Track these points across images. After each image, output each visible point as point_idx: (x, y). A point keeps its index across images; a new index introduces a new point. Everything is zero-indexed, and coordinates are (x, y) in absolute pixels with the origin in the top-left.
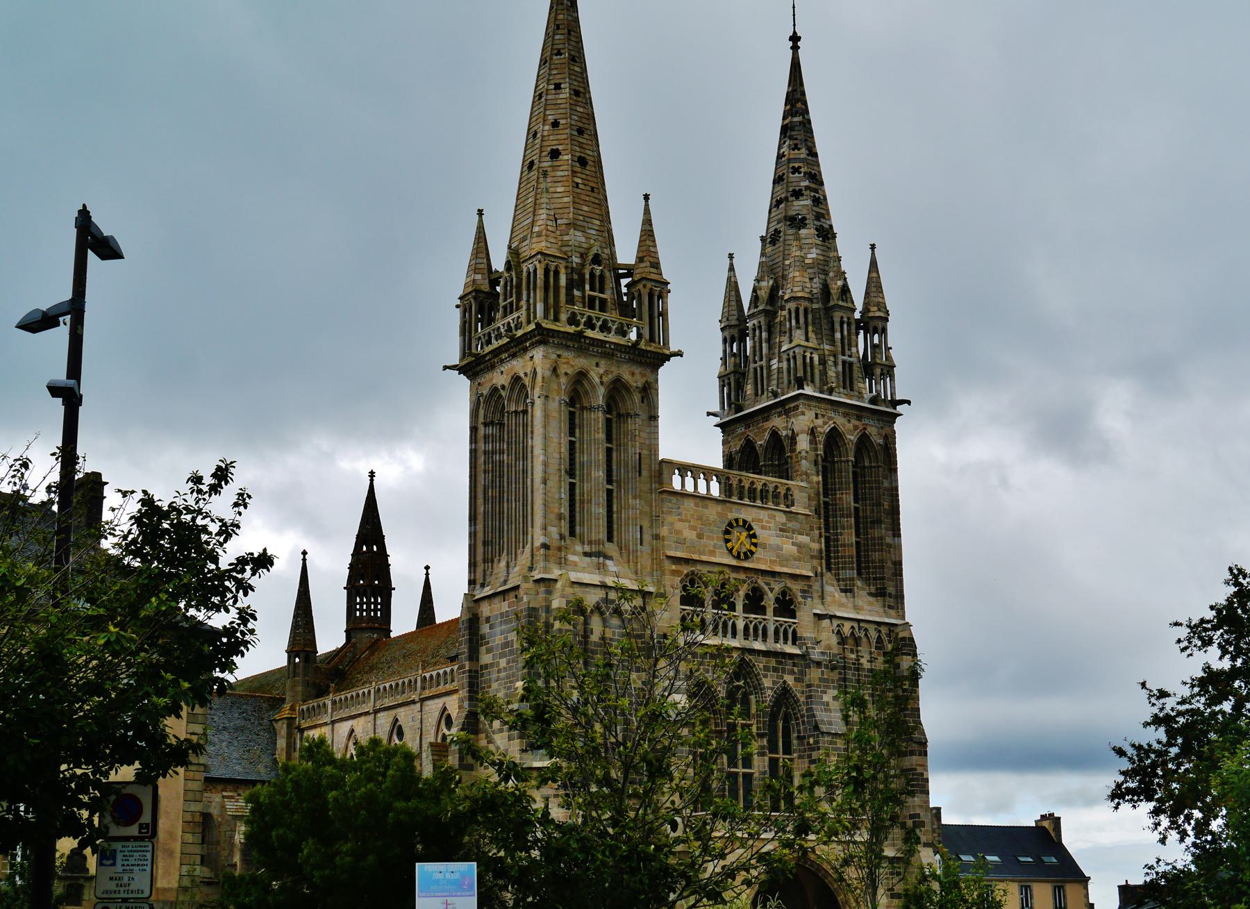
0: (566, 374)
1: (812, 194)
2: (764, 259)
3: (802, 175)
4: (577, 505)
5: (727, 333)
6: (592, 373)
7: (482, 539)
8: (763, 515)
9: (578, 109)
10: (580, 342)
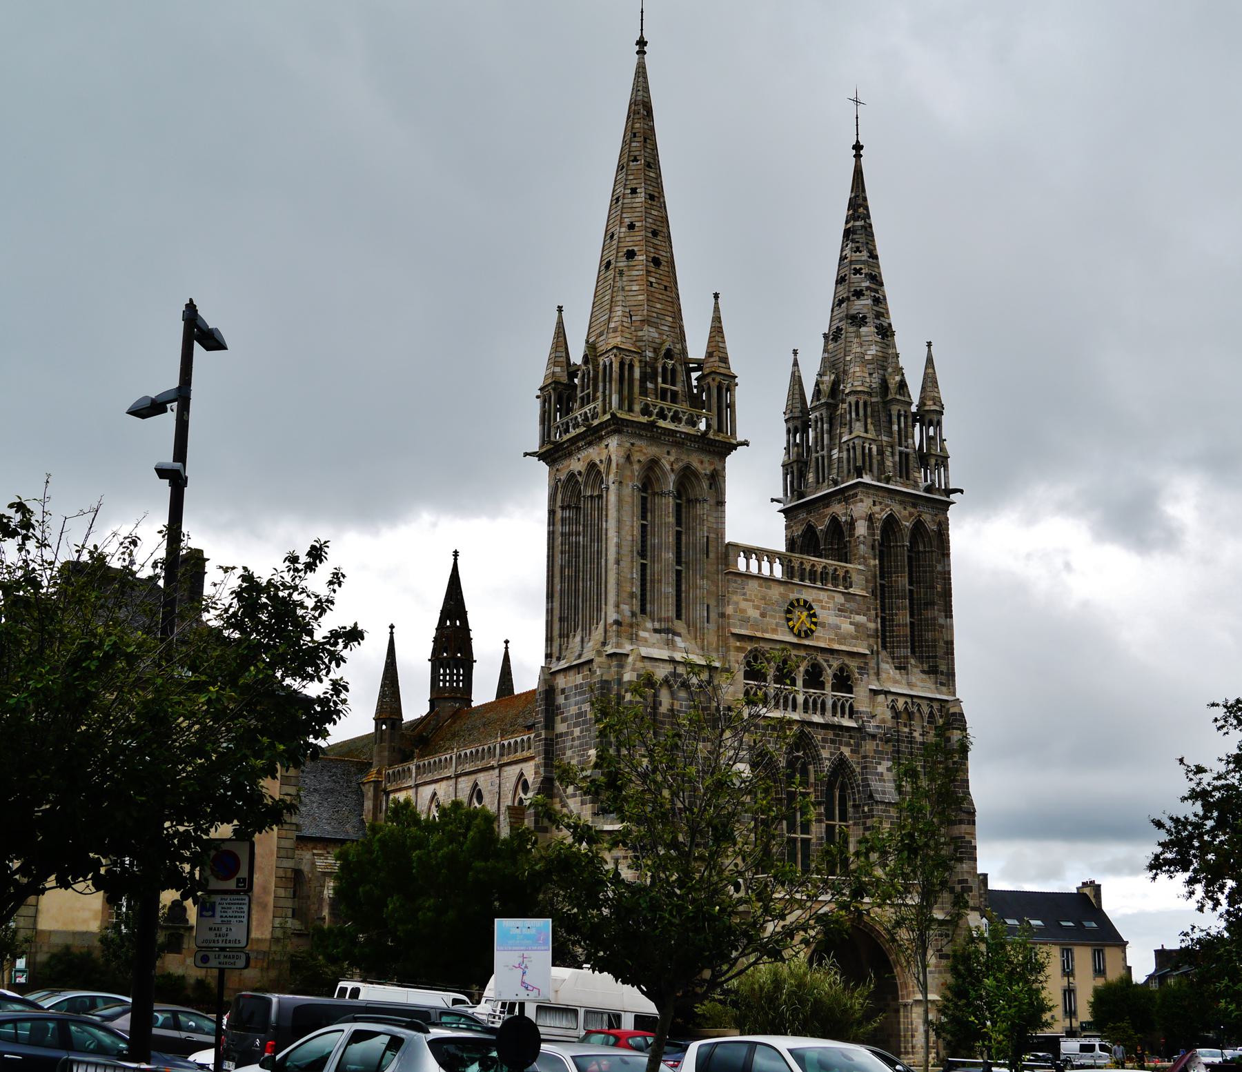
0: (639, 461)
1: (873, 294)
2: (826, 355)
3: (863, 276)
4: (648, 585)
5: (790, 425)
6: (663, 461)
7: (559, 616)
8: (823, 595)
9: (653, 212)
10: (652, 431)
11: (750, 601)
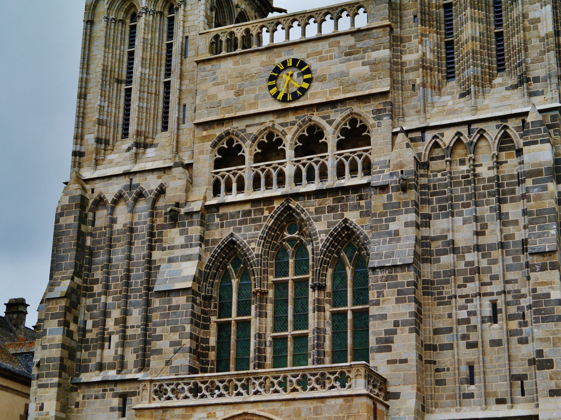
11: (223, 83)
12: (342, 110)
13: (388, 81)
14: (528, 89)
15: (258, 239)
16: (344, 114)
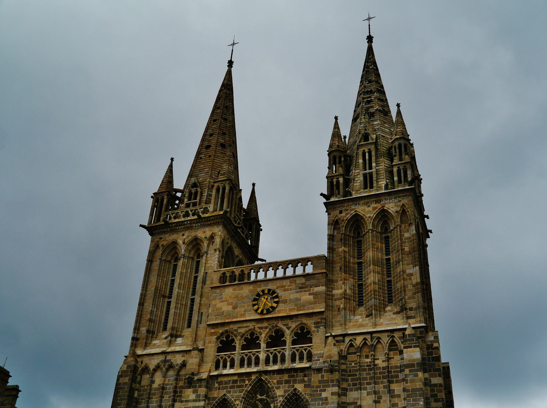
11: (226, 301)
12: (296, 321)
13: (324, 305)
14: (406, 314)
15: (241, 398)
16: (297, 324)
